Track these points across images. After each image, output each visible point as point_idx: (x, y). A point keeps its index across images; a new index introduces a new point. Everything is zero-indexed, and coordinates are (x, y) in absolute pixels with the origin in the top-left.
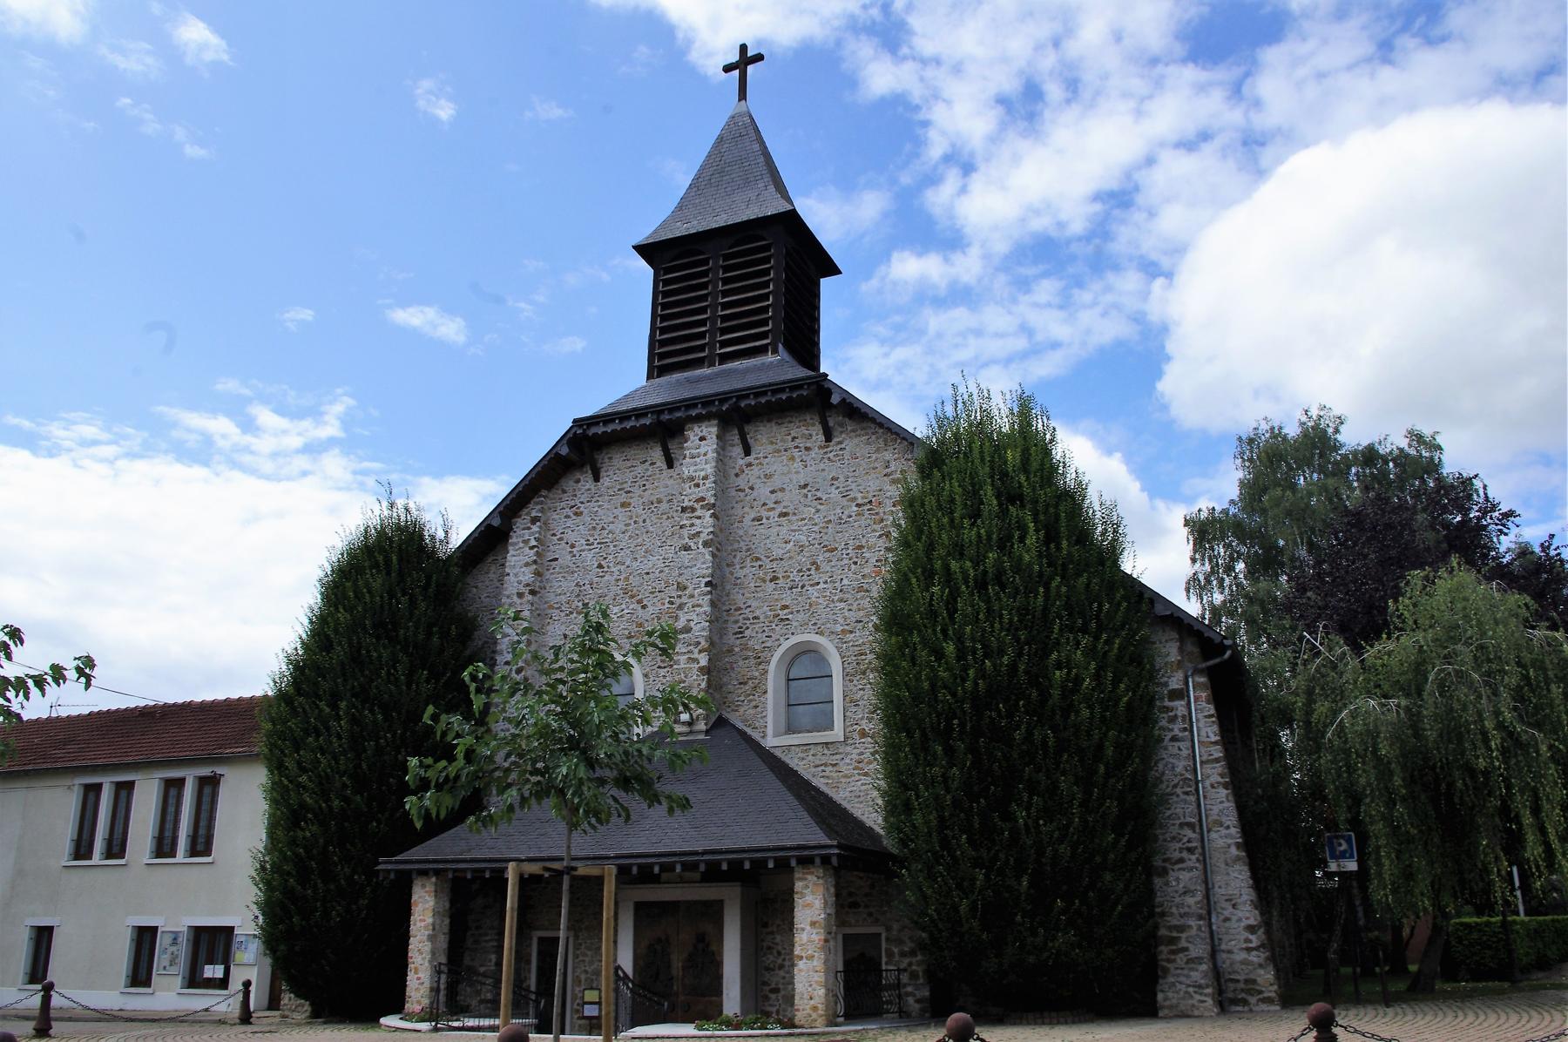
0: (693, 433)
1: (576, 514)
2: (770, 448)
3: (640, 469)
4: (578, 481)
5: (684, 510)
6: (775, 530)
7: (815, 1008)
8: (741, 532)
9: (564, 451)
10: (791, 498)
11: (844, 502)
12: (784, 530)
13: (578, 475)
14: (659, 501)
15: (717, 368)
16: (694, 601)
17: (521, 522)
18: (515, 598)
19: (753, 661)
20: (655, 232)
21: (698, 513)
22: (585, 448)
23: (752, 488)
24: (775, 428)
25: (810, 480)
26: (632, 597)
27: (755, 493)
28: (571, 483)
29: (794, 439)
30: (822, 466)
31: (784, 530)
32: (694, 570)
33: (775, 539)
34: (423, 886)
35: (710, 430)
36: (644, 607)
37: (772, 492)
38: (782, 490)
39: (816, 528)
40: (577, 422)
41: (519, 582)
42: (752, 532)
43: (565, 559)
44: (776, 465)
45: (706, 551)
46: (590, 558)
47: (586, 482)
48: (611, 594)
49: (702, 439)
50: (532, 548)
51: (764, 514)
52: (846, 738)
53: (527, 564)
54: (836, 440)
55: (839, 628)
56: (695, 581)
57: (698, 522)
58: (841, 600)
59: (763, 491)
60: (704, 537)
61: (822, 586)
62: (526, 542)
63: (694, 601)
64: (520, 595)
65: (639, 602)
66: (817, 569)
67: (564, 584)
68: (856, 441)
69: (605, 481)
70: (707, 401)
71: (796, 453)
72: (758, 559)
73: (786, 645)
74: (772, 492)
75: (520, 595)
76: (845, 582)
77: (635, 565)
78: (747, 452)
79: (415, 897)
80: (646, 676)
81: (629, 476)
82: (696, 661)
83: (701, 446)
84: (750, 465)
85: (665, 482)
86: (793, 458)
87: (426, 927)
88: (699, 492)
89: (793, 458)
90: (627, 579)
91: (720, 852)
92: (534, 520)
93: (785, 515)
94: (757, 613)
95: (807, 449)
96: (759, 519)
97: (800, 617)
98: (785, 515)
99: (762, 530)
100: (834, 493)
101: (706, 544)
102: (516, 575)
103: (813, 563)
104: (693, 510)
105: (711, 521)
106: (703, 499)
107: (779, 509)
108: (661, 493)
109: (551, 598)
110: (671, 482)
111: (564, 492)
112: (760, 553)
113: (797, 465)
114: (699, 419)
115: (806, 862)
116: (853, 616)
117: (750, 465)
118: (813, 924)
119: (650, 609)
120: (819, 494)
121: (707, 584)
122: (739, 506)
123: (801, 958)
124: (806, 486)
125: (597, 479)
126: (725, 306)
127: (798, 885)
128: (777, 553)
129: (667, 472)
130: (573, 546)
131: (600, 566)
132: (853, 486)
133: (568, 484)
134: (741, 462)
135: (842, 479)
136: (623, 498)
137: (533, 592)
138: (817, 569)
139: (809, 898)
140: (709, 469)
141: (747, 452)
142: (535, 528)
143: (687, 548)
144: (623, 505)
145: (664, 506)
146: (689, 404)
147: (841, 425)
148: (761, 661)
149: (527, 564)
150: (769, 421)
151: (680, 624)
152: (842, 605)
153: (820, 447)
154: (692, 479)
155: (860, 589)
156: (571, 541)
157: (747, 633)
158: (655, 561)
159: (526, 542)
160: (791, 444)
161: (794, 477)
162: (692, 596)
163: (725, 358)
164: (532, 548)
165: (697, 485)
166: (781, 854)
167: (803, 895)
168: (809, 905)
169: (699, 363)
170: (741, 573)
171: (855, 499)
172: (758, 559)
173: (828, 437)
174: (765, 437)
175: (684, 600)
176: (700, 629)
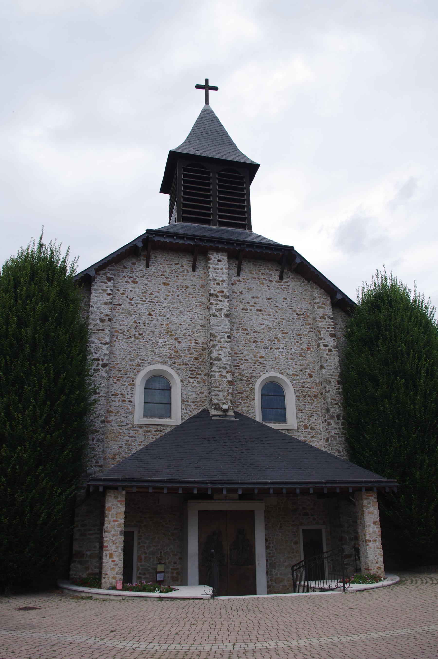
0: (214, 257)
1: (133, 282)
2: (250, 276)
3: (174, 267)
4: (134, 264)
5: (211, 295)
6: (255, 317)
7: (379, 568)
8: (236, 314)
9: (140, 245)
10: (263, 303)
11: (290, 311)
12: (260, 318)
13: (134, 261)
14: (187, 287)
15: (217, 227)
16: (221, 344)
17: (100, 278)
18: (98, 322)
19: (245, 382)
20: (179, 148)
21: (220, 298)
22: (147, 247)
23: (241, 293)
24: (252, 266)
25: (272, 296)
26: (171, 335)
27: (243, 296)
28: (130, 264)
29: (263, 274)
30: (278, 291)
31: (260, 318)
32: (220, 328)
33: (255, 321)
34: (116, 497)
35: (225, 258)
36: (179, 342)
37: (253, 297)
38: (257, 298)
39: (276, 321)
40: (148, 231)
41: (101, 313)
42: (242, 315)
43: (126, 305)
44: (253, 284)
45: (226, 319)
46: (143, 308)
47: (140, 266)
48: (158, 332)
49: (219, 261)
50: (109, 294)
51: (249, 308)
52: (298, 428)
53: (106, 303)
54: (284, 280)
55: (291, 373)
56: (221, 334)
57: (220, 303)
58: (291, 359)
59: (247, 296)
60: (224, 311)
61: (281, 350)
62: (105, 290)
63: (221, 344)
64: (102, 321)
65: (176, 339)
66: (278, 341)
67: (126, 320)
68: (294, 283)
69: (152, 269)
70: (230, 242)
71: (264, 281)
72: (246, 330)
73: (264, 377)
74: (253, 297)
75: (102, 321)
76: (293, 350)
77: (173, 318)
78: (238, 274)
79: (108, 505)
80: (182, 381)
81: (168, 270)
82: (225, 377)
83: (219, 266)
84: (239, 281)
85: (192, 279)
86: (263, 283)
87: (119, 526)
88: (219, 288)
89: (263, 283)
90: (168, 325)
91: (335, 483)
92: (109, 279)
93: (260, 310)
94: (247, 357)
95: (270, 281)
96: (246, 309)
97: (271, 363)
98: (260, 310)
99: (247, 315)
100: (285, 306)
101: (226, 316)
102: (98, 308)
103: (276, 338)
104: (217, 296)
105: (228, 304)
106: (222, 292)
107: (257, 307)
108: (189, 283)
109: (117, 326)
110: (194, 279)
111: (125, 268)
112: (247, 326)
113: (265, 287)
114: (217, 250)
115: (369, 489)
116: (298, 368)
117: (239, 281)
118: (374, 523)
119: (183, 344)
120: (277, 304)
121: (229, 337)
122: (235, 300)
123: (370, 541)
124: (270, 299)
125: (147, 266)
126: (220, 198)
127: (365, 502)
128: (256, 328)
129: (191, 273)
130: (131, 299)
131: (150, 314)
132: (294, 305)
133: (128, 264)
134: (234, 278)
135: (288, 299)
136: (164, 280)
137: (110, 320)
138: (278, 341)
139: (371, 509)
140: (225, 277)
141: (238, 274)
142: (110, 284)
143: (215, 316)
144: (164, 284)
145: (190, 290)
146: (221, 241)
147: (287, 274)
148: (250, 382)
149: (106, 303)
150: (249, 262)
151: (214, 355)
152: (292, 361)
153: (277, 282)
154: (215, 280)
155: (301, 355)
156: (131, 295)
157: (241, 367)
158: (186, 319)
159: (105, 290)
160: (261, 276)
161: (264, 293)
162: (220, 342)
163: (222, 224)
164: (109, 294)
165: (219, 284)
166: (343, 485)
167: (368, 507)
168: (371, 513)
169: (208, 222)
170: (237, 335)
171: (295, 311)
172: (246, 330)
173: (281, 278)
174: (248, 270)
175: (216, 343)
176: (225, 360)
